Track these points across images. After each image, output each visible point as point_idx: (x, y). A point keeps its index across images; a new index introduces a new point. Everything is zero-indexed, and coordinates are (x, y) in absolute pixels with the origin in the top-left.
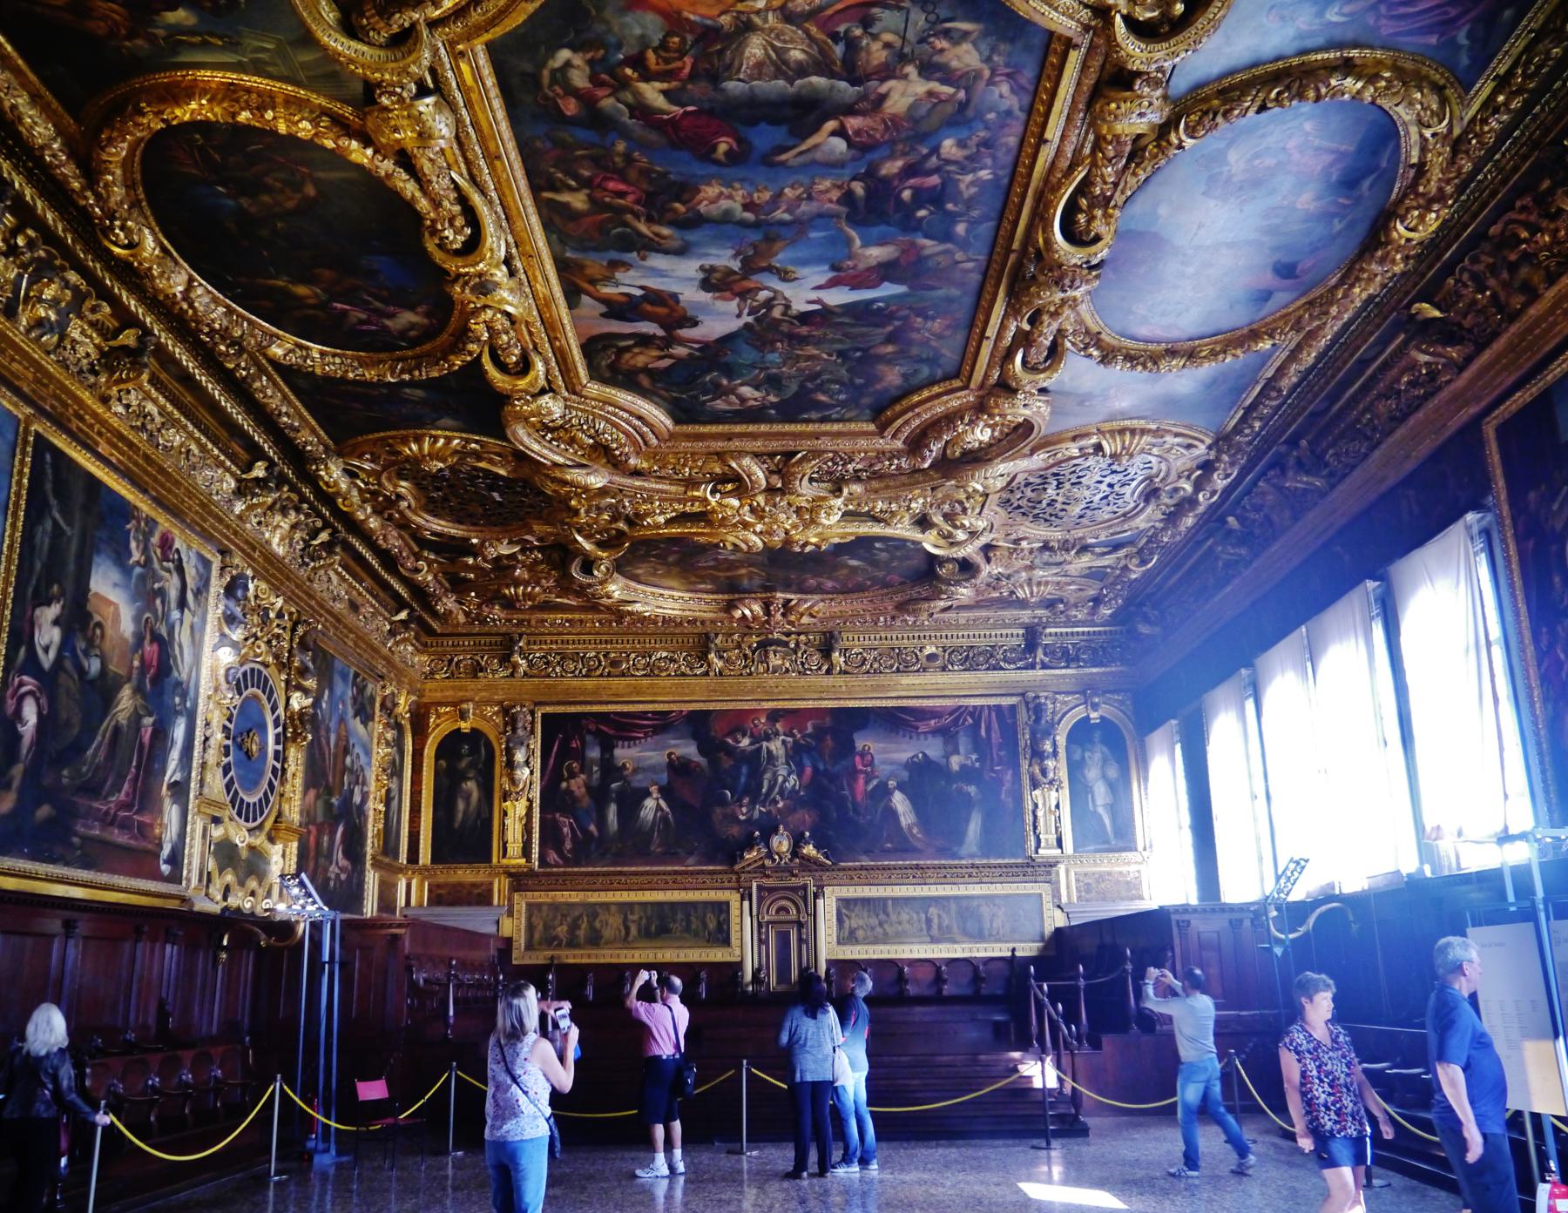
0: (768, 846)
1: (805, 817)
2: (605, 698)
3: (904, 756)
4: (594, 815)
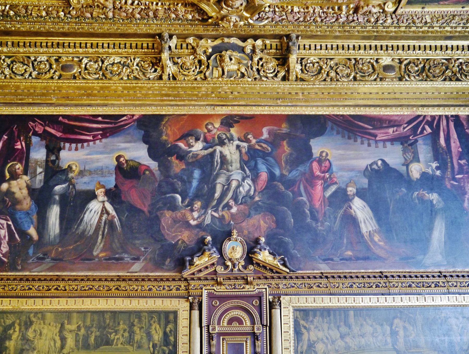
0: (220, 251)
1: (261, 224)
2: (54, 101)
3: (363, 163)
4: (35, 217)
